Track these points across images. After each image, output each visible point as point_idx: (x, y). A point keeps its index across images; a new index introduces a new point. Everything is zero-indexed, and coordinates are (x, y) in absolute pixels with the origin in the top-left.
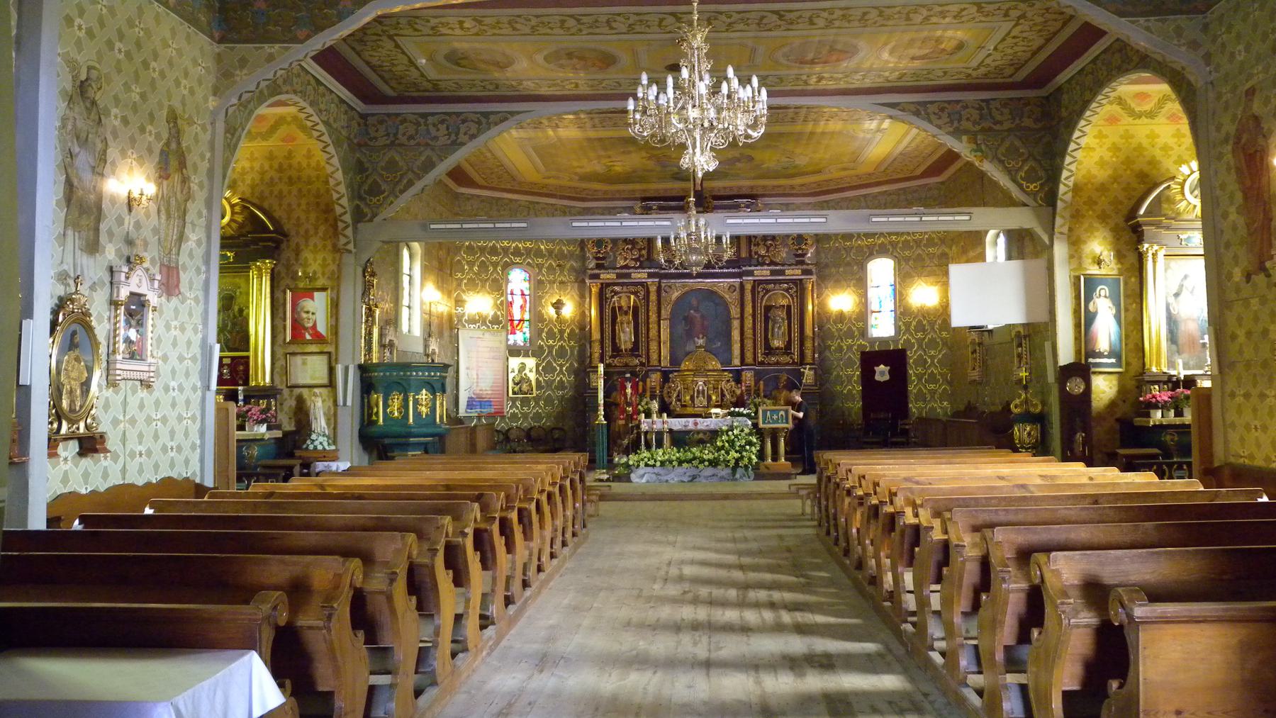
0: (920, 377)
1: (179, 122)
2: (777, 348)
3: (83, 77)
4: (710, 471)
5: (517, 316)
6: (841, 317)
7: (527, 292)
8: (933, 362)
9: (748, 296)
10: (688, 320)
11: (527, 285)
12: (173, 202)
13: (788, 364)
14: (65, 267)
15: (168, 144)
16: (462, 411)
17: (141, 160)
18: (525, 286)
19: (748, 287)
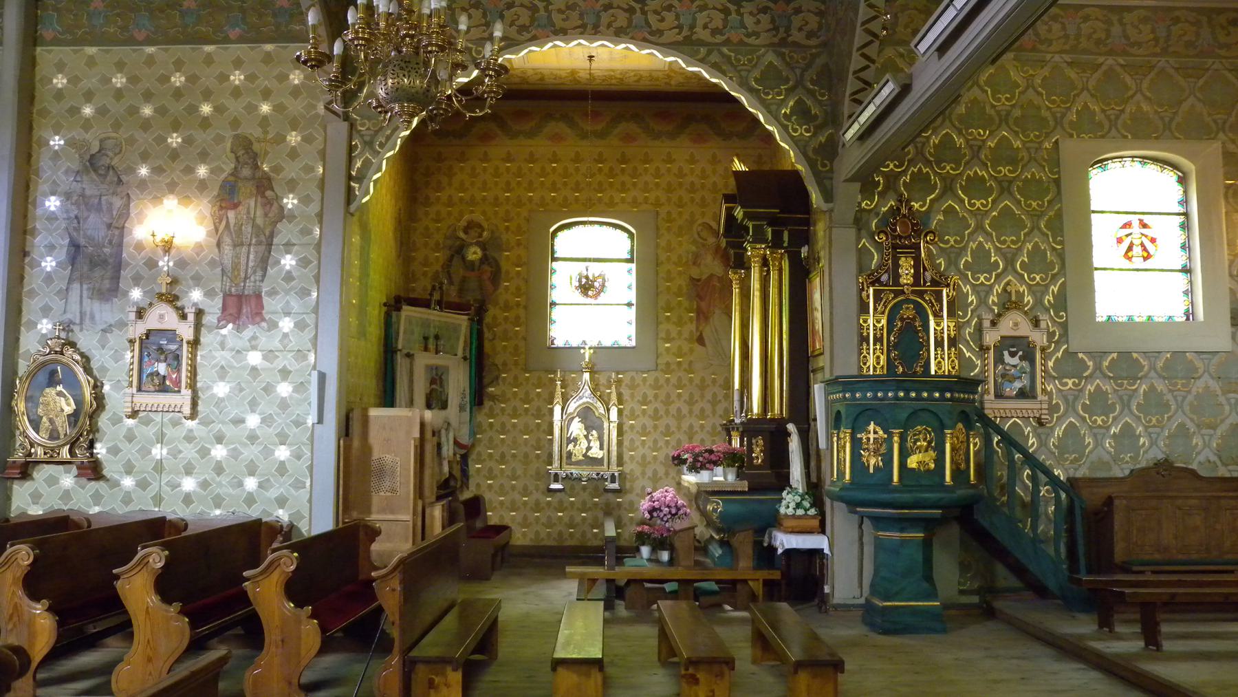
1: (256, 147)
3: (95, 148)
12: (247, 229)
14: (69, 316)
15: (235, 173)
17: (185, 199)
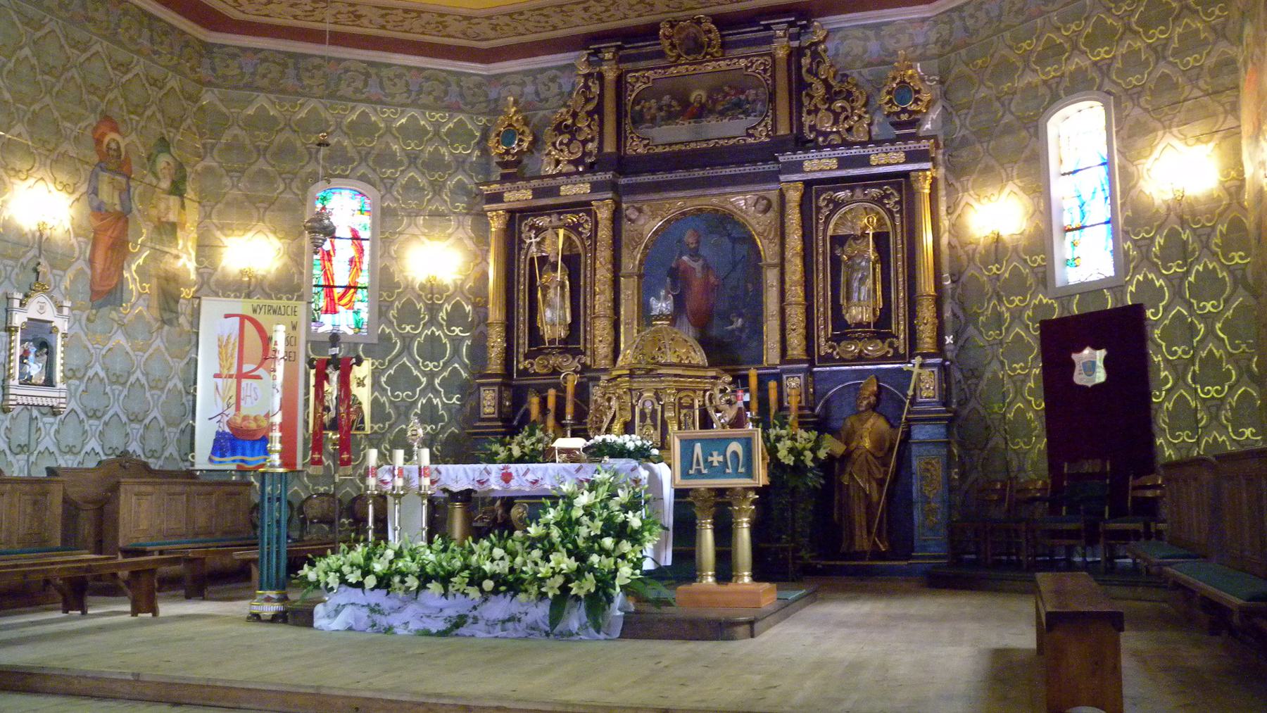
0: (1179, 370)
2: (860, 325)
4: (499, 608)
5: (342, 276)
6: (997, 249)
7: (365, 234)
8: (1210, 331)
9: (794, 217)
10: (678, 278)
11: (366, 220)
13: (884, 359)
16: (202, 458)
18: (363, 224)
19: (794, 196)
